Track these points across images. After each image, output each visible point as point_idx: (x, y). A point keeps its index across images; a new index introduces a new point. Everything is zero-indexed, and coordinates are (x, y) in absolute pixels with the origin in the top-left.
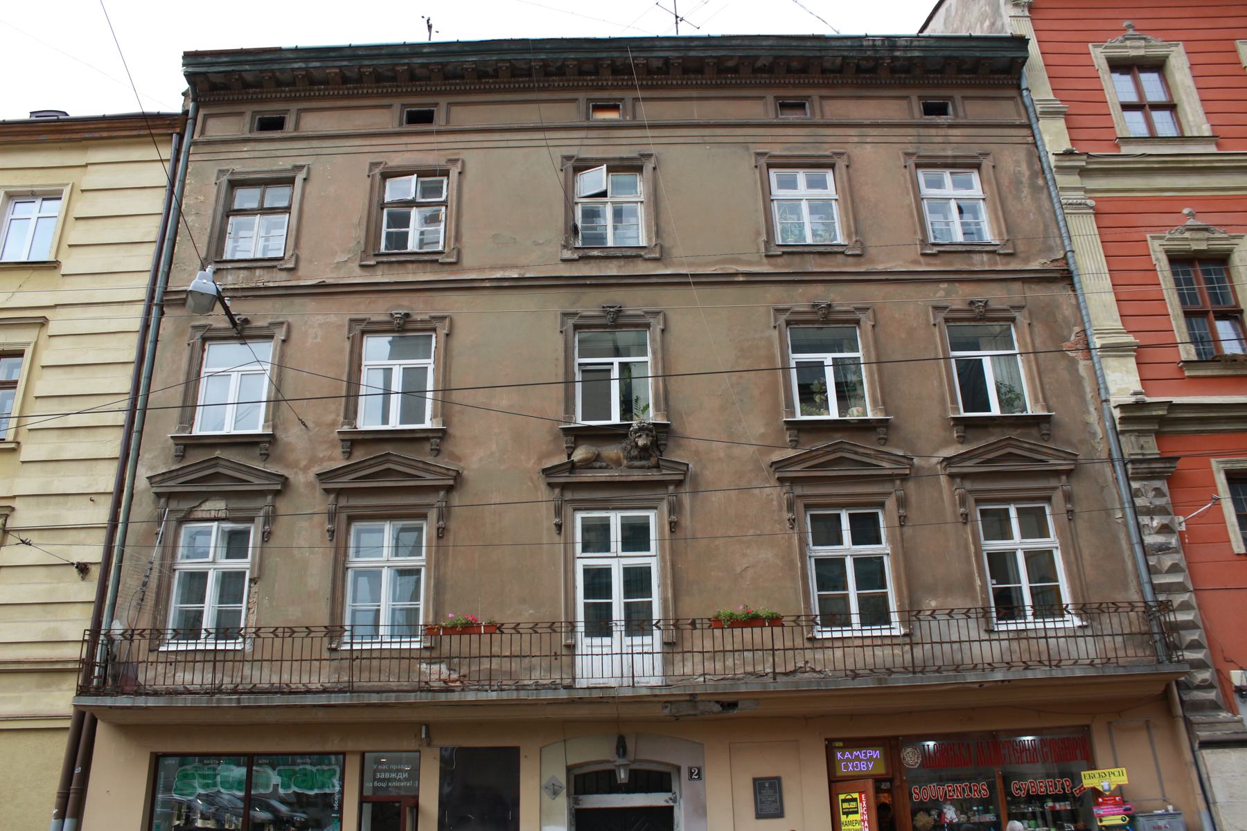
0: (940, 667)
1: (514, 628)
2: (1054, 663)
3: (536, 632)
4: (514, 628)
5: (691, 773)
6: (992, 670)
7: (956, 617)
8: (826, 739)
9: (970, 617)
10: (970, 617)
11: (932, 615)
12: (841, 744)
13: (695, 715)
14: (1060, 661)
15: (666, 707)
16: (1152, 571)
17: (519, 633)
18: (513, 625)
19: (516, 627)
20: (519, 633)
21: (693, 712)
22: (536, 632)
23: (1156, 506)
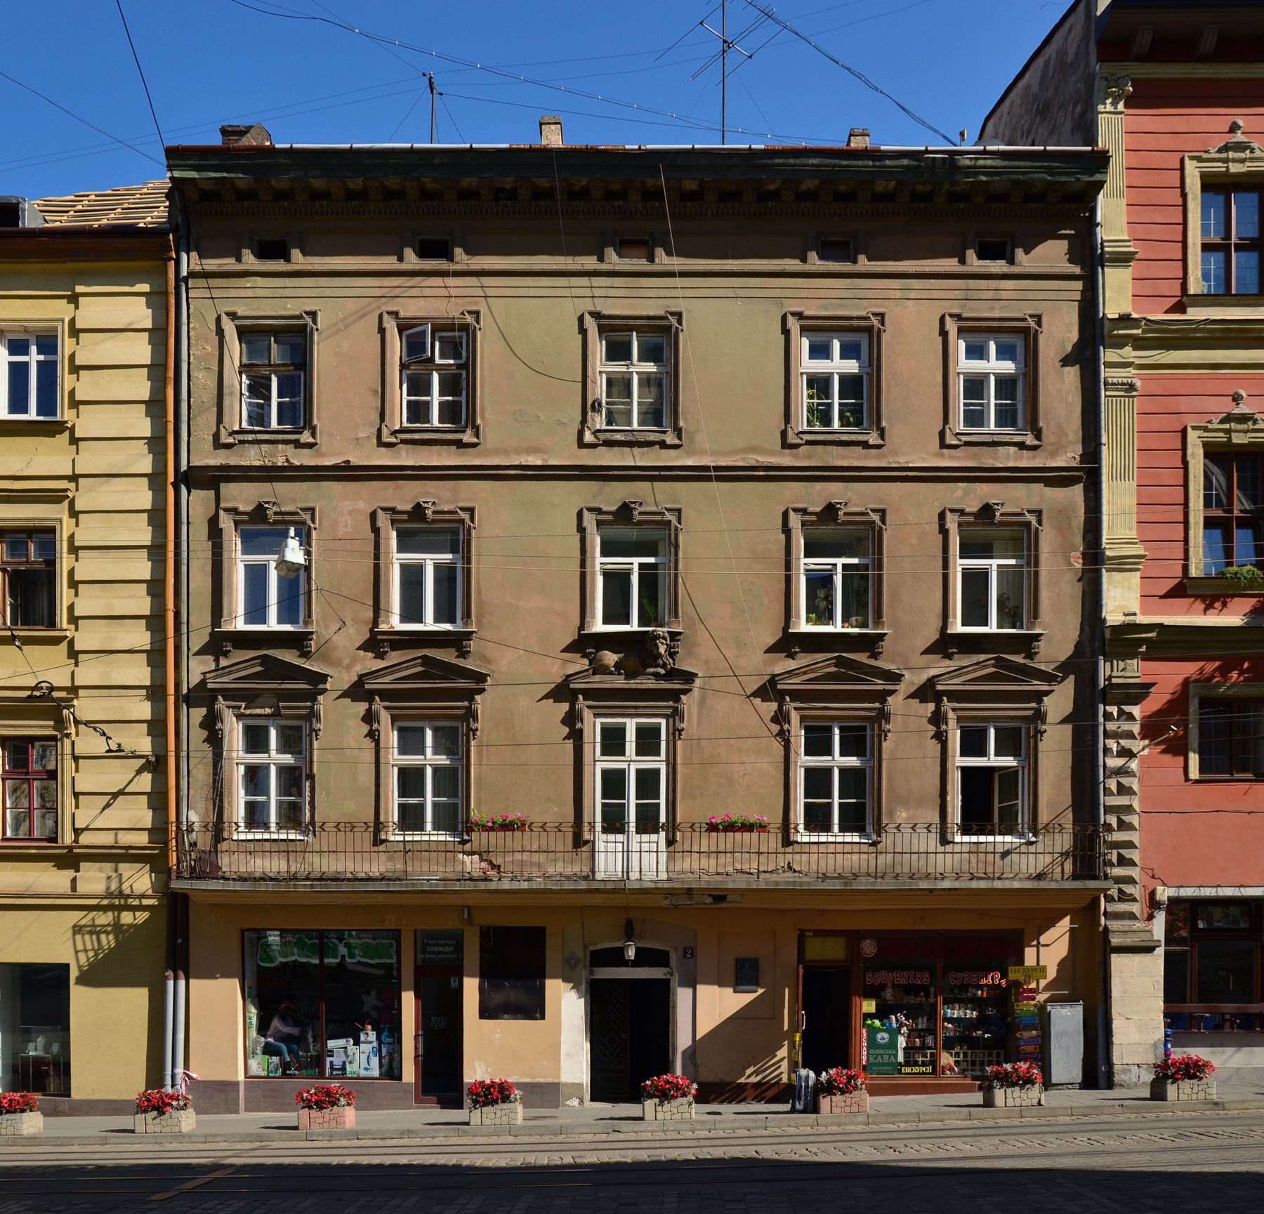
0: (898, 874)
1: (542, 827)
2: (997, 875)
3: (560, 831)
4: (542, 827)
5: (686, 953)
6: (942, 879)
7: (918, 830)
8: (799, 930)
9: (930, 831)
10: (930, 831)
11: (898, 828)
12: (811, 934)
13: (691, 905)
14: (1003, 874)
15: (667, 898)
16: (1107, 793)
17: (545, 831)
18: (541, 825)
19: (543, 826)
20: (545, 831)
21: (689, 903)
22: (560, 831)
23: (1123, 731)
